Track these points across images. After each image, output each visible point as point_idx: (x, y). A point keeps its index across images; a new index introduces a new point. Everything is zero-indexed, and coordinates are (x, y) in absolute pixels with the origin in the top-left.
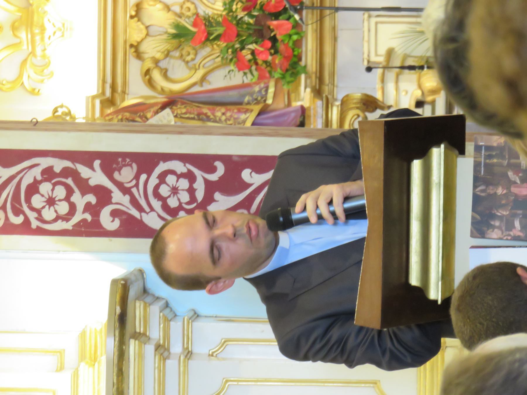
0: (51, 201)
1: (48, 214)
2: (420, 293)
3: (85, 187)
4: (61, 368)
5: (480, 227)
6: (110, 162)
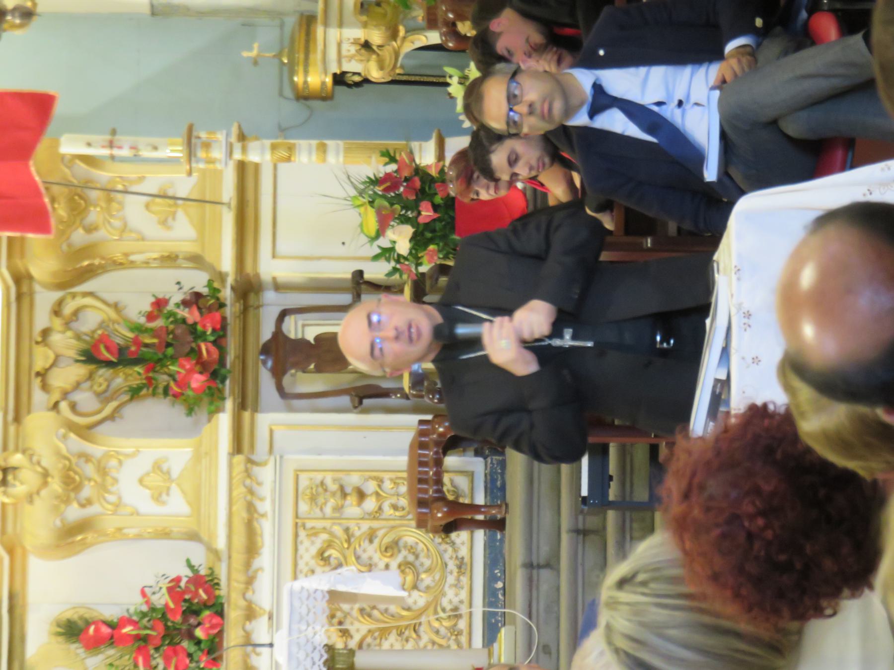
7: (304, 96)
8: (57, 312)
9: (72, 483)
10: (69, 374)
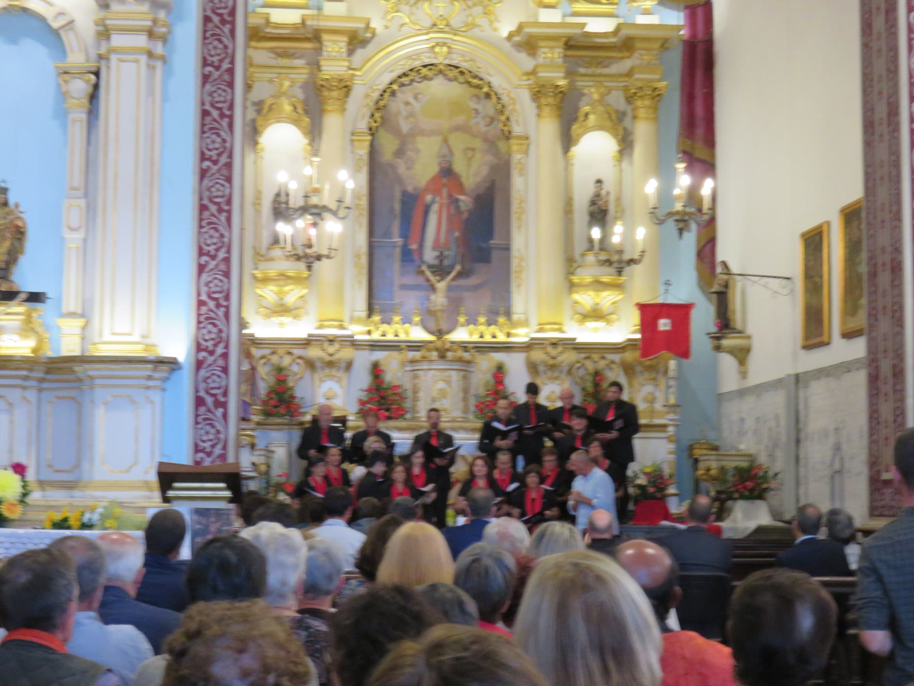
0: (210, 333)
1: (205, 331)
2: (171, 488)
3: (216, 345)
4: (143, 337)
5: (199, 512)
6: (225, 356)
7: (691, 448)
8: (613, 362)
9: (553, 367)
10: (590, 366)
